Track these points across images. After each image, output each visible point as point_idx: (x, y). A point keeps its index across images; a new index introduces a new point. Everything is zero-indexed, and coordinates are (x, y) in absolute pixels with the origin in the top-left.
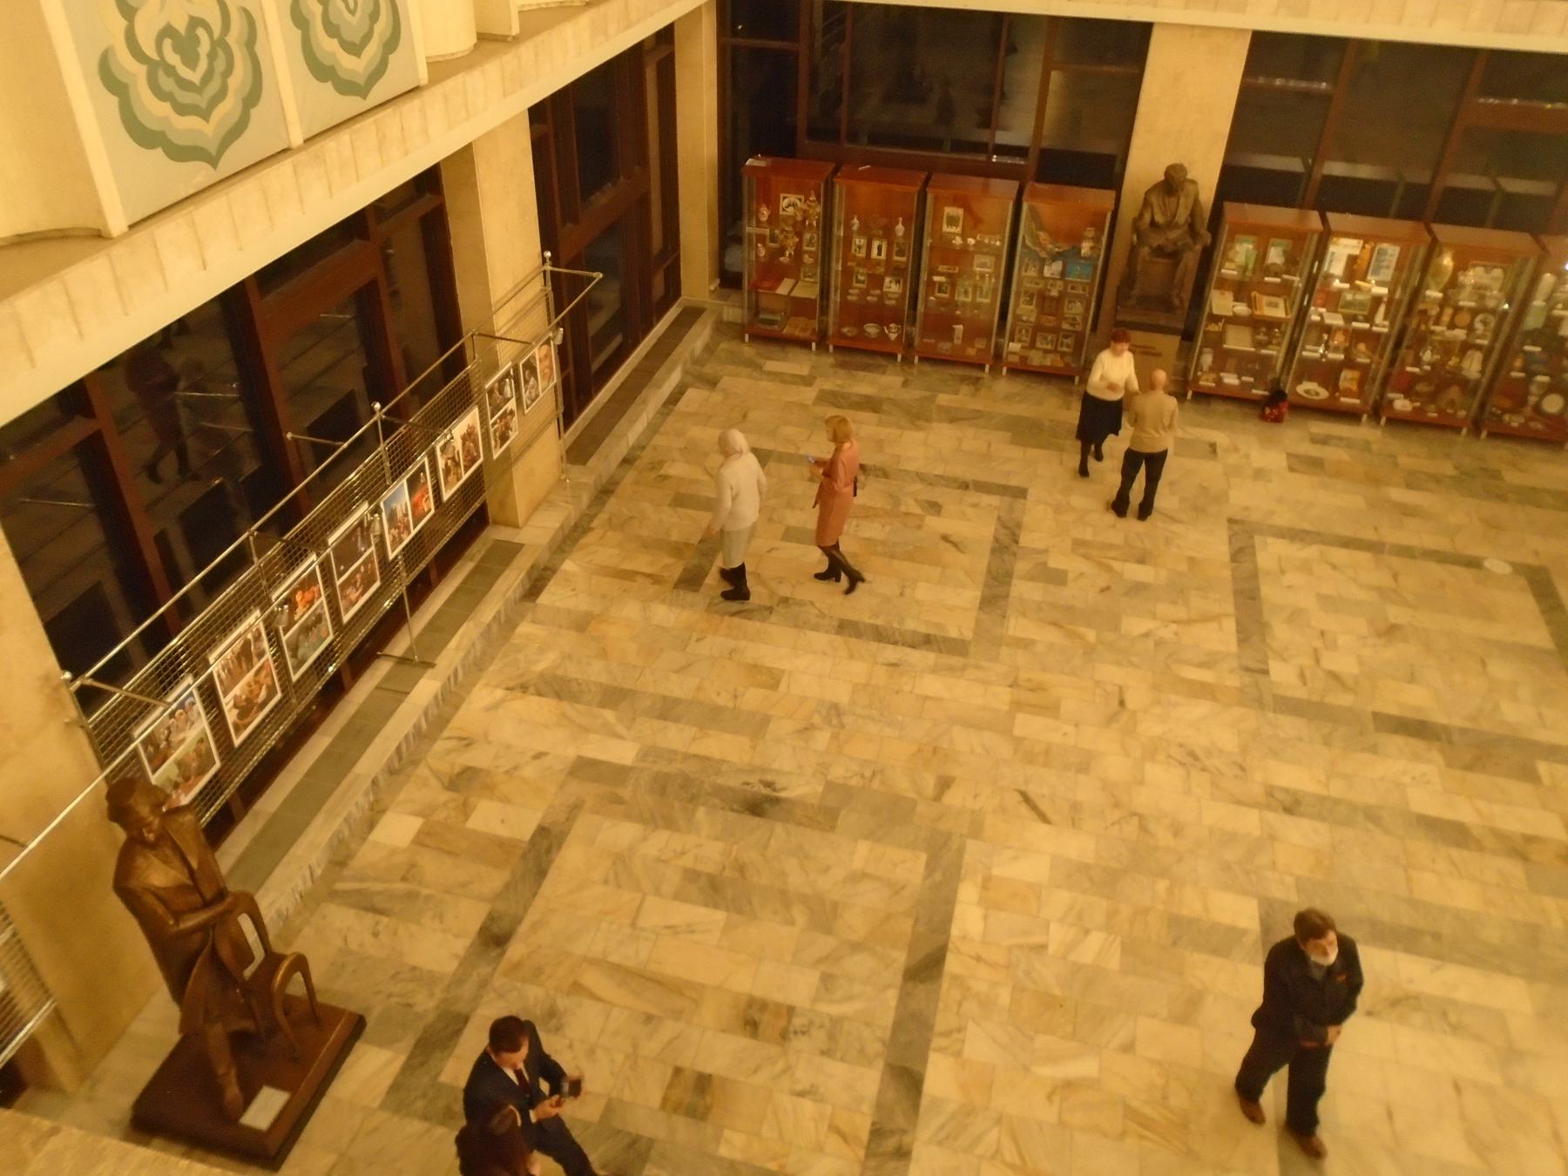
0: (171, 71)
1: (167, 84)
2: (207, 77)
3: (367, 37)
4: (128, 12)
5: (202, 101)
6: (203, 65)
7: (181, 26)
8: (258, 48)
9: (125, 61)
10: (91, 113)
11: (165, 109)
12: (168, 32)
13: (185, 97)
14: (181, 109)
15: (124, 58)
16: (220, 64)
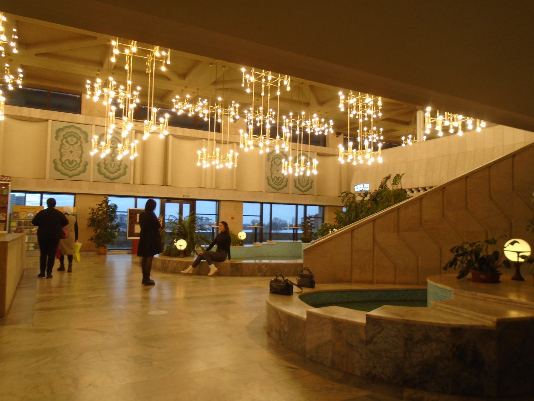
0: (66, 164)
1: (64, 165)
2: (74, 167)
3: (116, 172)
4: (61, 156)
5: (71, 169)
6: (73, 165)
7: (71, 160)
8: (88, 167)
9: (58, 161)
10: (49, 164)
11: (63, 168)
12: (68, 160)
13: (66, 167)
14: (65, 169)
15: (58, 161)
16: (77, 166)
